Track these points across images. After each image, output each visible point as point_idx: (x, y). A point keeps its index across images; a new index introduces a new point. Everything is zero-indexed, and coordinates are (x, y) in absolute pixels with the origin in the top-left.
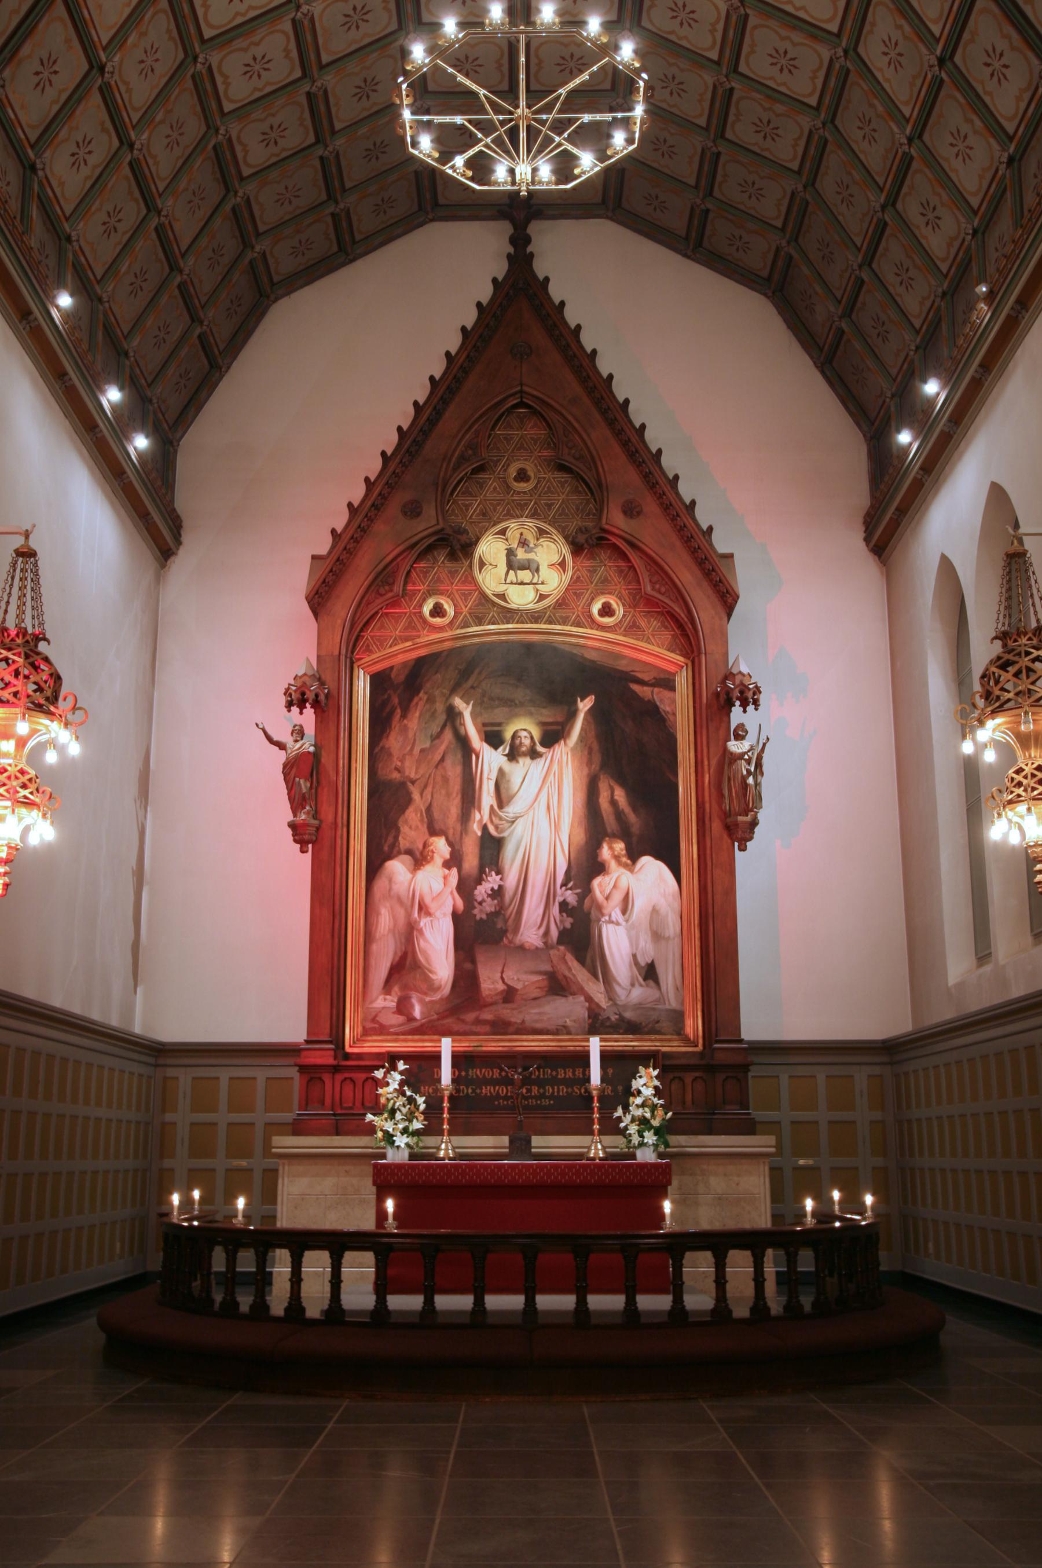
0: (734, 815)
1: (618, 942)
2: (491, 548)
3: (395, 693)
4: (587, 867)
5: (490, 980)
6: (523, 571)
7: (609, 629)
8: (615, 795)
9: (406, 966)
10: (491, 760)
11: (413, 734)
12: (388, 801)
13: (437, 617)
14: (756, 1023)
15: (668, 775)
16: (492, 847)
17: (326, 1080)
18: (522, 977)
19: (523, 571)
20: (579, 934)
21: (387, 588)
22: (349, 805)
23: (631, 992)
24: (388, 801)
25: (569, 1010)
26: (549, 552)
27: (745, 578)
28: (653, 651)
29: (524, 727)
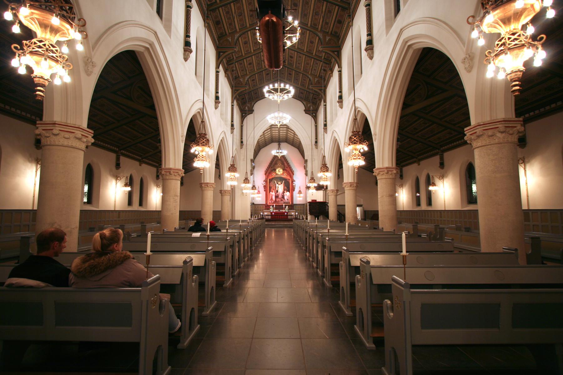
0: (293, 189)
1: (286, 197)
2: (277, 170)
3: (271, 180)
4: (284, 192)
5: (277, 200)
6: (279, 172)
7: (285, 176)
8: (286, 188)
9: (272, 199)
10: (277, 185)
11: (272, 183)
12: (270, 188)
13: (274, 175)
14: (294, 203)
15: (289, 187)
16: (277, 191)
17: (267, 207)
18: (279, 200)
19: (279, 172)
20: (283, 197)
21: (270, 173)
22: (268, 188)
23: (286, 201)
24: (270, 188)
25: (282, 202)
26: (281, 170)
27: (295, 173)
28: (288, 177)
29: (279, 183)
